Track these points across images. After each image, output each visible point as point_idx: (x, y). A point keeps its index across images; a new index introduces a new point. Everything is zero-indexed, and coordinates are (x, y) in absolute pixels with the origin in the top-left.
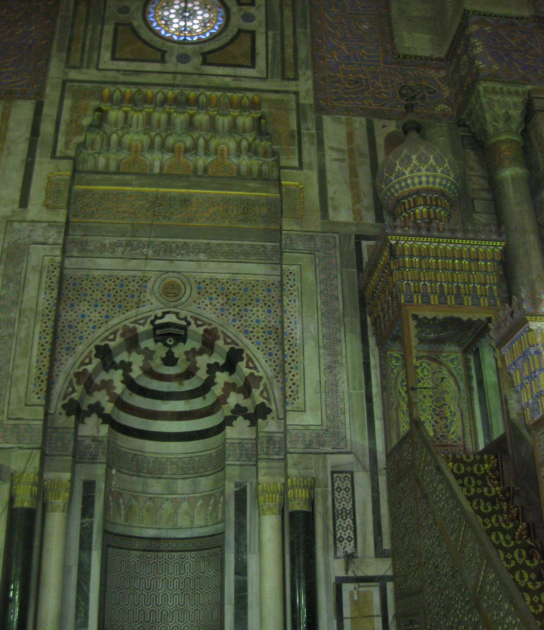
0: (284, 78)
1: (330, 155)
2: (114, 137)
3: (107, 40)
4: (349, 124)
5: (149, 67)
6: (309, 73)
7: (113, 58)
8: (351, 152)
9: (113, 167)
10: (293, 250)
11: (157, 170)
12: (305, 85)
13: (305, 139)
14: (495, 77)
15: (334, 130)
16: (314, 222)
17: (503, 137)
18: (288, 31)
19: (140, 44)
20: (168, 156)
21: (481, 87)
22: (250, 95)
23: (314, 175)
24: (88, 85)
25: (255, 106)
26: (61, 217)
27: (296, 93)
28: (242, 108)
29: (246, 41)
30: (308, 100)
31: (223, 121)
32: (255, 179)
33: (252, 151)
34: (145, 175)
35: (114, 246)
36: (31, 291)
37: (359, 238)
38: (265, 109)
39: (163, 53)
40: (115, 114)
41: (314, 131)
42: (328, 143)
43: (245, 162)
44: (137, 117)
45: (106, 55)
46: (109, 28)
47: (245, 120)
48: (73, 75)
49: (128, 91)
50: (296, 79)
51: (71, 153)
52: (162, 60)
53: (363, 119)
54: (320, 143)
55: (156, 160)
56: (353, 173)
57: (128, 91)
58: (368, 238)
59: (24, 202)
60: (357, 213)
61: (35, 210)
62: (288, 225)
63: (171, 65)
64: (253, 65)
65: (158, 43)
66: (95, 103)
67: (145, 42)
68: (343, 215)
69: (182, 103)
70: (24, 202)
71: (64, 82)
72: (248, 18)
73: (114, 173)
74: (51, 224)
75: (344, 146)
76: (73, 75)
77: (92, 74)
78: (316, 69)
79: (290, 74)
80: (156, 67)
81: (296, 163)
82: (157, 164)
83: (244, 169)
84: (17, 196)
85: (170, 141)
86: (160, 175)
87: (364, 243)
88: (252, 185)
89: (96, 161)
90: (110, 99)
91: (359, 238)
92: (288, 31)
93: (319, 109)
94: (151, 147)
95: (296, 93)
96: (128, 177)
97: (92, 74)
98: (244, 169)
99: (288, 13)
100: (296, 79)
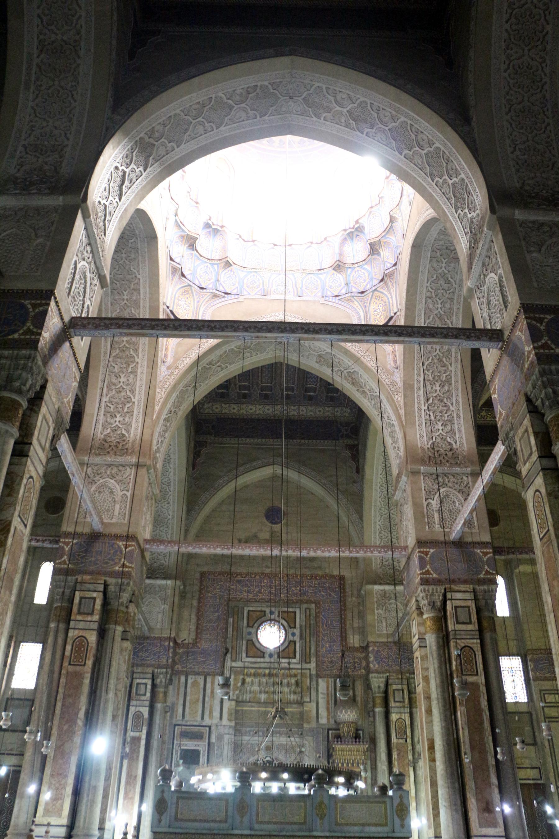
0: (306, 663)
1: (320, 696)
2: (248, 688)
3: (244, 648)
4: (328, 683)
5: (258, 660)
6: (315, 660)
7: (247, 657)
8: (328, 694)
9: (248, 700)
10: (307, 735)
11: (263, 701)
12: (313, 665)
13: (312, 690)
14: (377, 672)
15: (322, 684)
16: (314, 725)
17: (377, 695)
18: (308, 640)
19: (256, 650)
20: (266, 695)
21: (371, 675)
22: (294, 671)
23: (314, 705)
24: (239, 669)
25: (295, 676)
26: (233, 724)
27: (310, 669)
28: (291, 676)
29: (292, 644)
30: (314, 672)
31: (285, 681)
32: (295, 703)
33: (295, 693)
34: (259, 702)
35: (250, 731)
36: (225, 752)
37: (329, 730)
38: (299, 677)
39: (264, 653)
40: (248, 680)
41: (315, 686)
42: (320, 690)
43: (293, 697)
44: (256, 680)
45: (244, 655)
46: (244, 642)
47: (293, 681)
48: (234, 664)
49: (253, 671)
50: (310, 663)
51: (235, 698)
52: (264, 657)
53: (333, 679)
54: (317, 691)
55: (263, 697)
56: (328, 703)
57: (253, 671)
58: (331, 729)
59: (221, 718)
60: (328, 719)
61: (225, 721)
62: (305, 726)
63: (267, 659)
64: (295, 658)
65: (262, 649)
66: (241, 677)
67: (257, 649)
68: (323, 721)
69: (270, 675)
70: (221, 718)
71: (231, 668)
72: (293, 634)
73: (249, 702)
74: (230, 727)
75: (325, 692)
76: (234, 664)
77: (239, 664)
78: (317, 656)
79: (308, 661)
80: (262, 660)
81: (309, 700)
82: (263, 698)
83: (292, 700)
84: (219, 716)
85: (267, 689)
86: (264, 702)
87: (330, 732)
88: (295, 706)
89: (243, 697)
90: (247, 675)
91: (329, 730)
92: (308, 640)
93: (318, 676)
94: (260, 692)
95: (310, 669)
96: (253, 704)
97: (239, 664)
98: (292, 700)
99: (308, 631)
100: (310, 663)
